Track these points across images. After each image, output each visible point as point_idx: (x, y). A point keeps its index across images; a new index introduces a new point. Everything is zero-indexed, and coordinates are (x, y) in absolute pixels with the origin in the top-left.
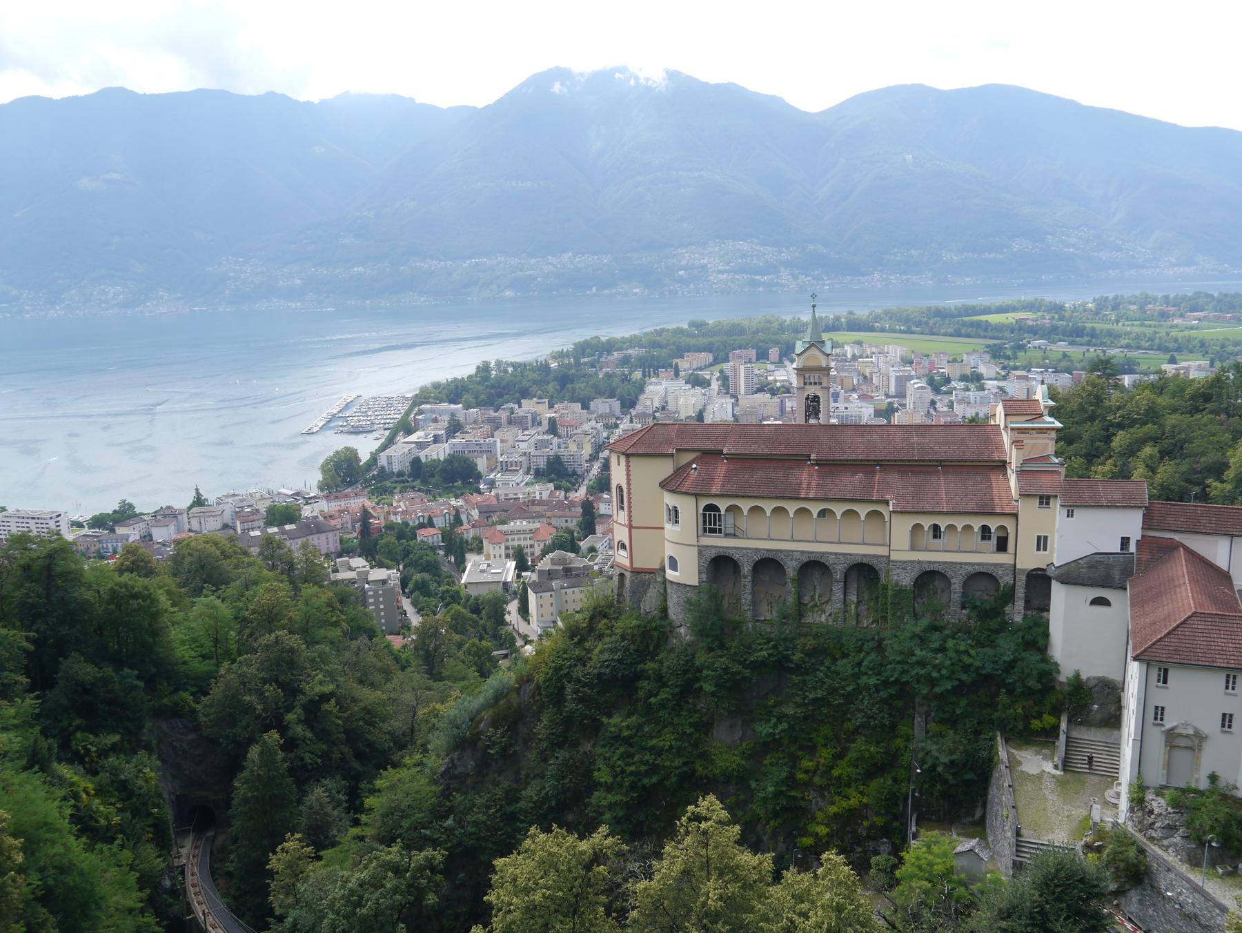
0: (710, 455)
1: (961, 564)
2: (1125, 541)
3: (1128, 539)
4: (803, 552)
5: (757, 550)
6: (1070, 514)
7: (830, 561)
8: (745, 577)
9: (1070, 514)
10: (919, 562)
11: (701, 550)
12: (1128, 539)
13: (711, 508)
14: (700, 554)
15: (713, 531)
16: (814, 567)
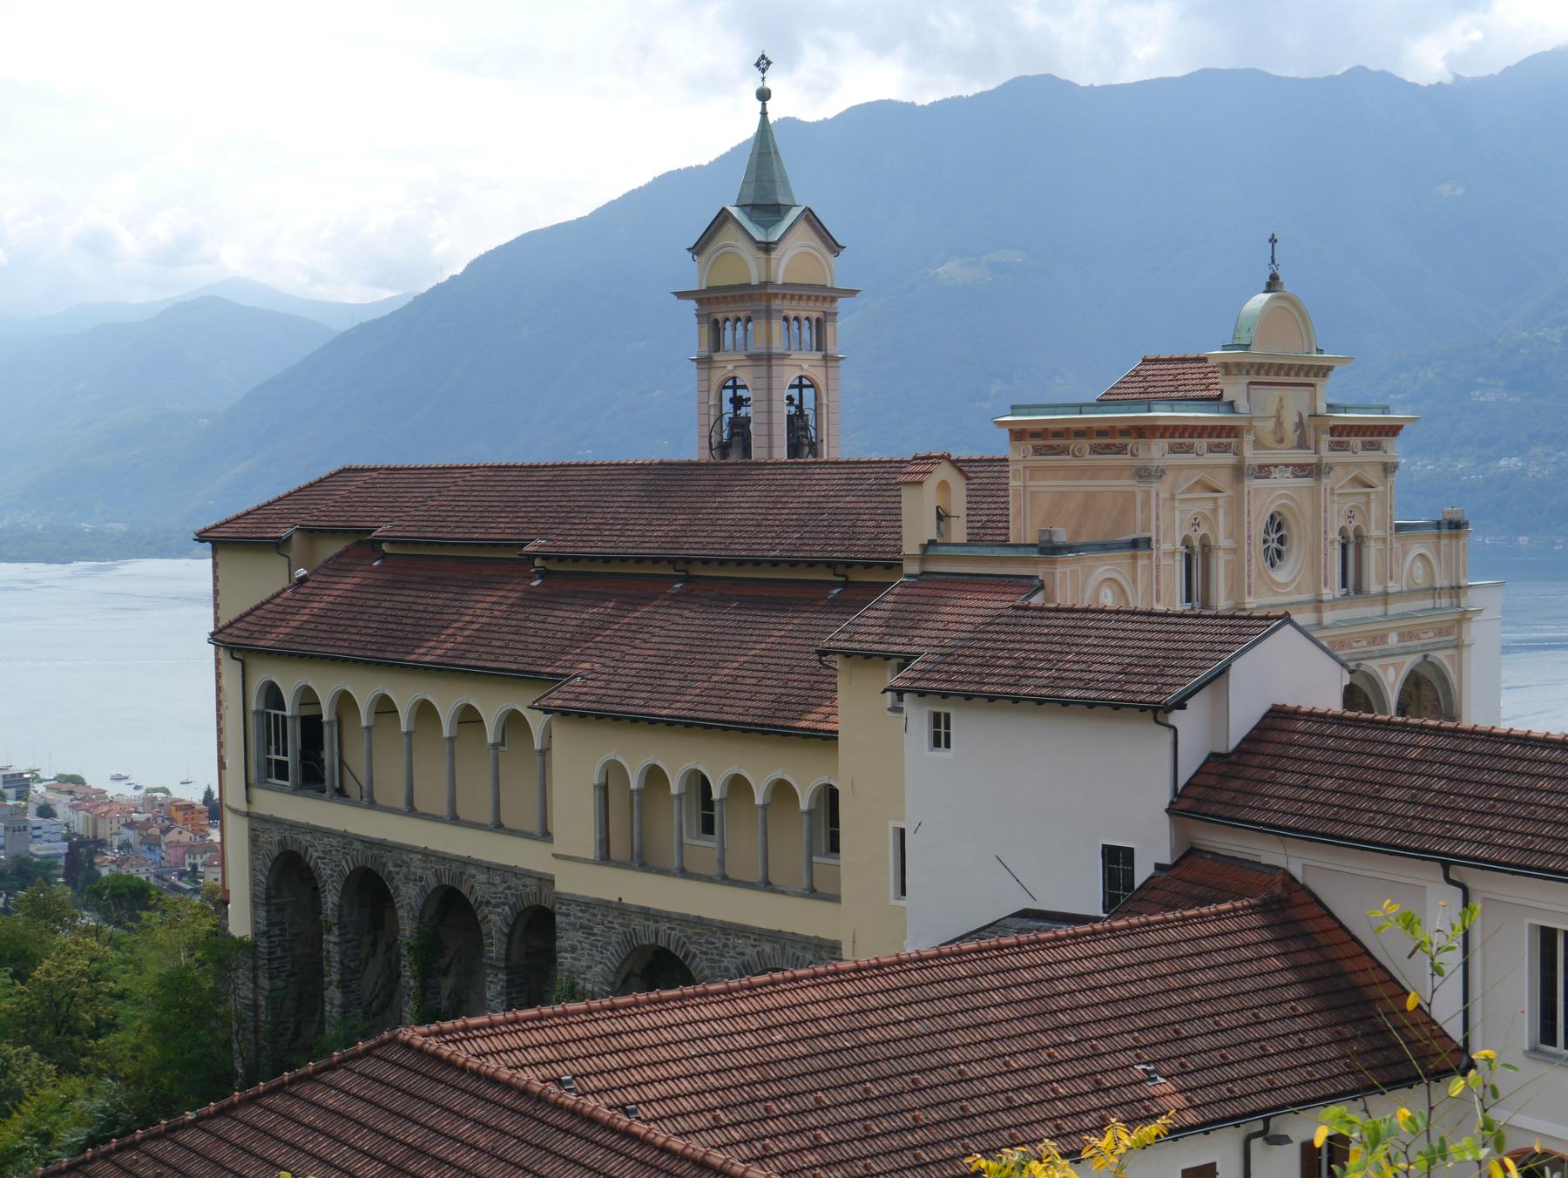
0: (364, 543)
1: (727, 929)
2: (1117, 860)
3: (1129, 853)
4: (426, 854)
5: (347, 838)
6: (940, 739)
7: (478, 889)
8: (329, 931)
9: (940, 739)
10: (621, 909)
11: (259, 824)
12: (1129, 853)
13: (273, 695)
14: (254, 840)
15: (282, 771)
16: (451, 903)
